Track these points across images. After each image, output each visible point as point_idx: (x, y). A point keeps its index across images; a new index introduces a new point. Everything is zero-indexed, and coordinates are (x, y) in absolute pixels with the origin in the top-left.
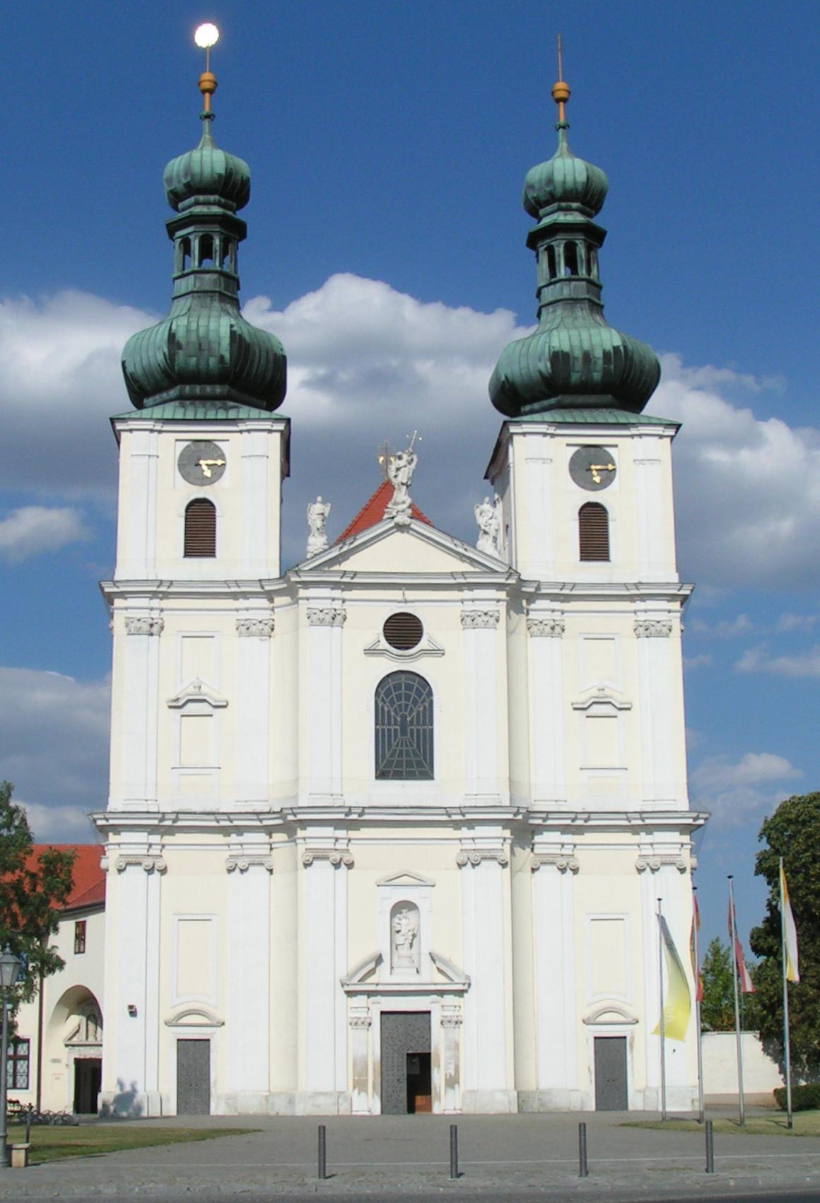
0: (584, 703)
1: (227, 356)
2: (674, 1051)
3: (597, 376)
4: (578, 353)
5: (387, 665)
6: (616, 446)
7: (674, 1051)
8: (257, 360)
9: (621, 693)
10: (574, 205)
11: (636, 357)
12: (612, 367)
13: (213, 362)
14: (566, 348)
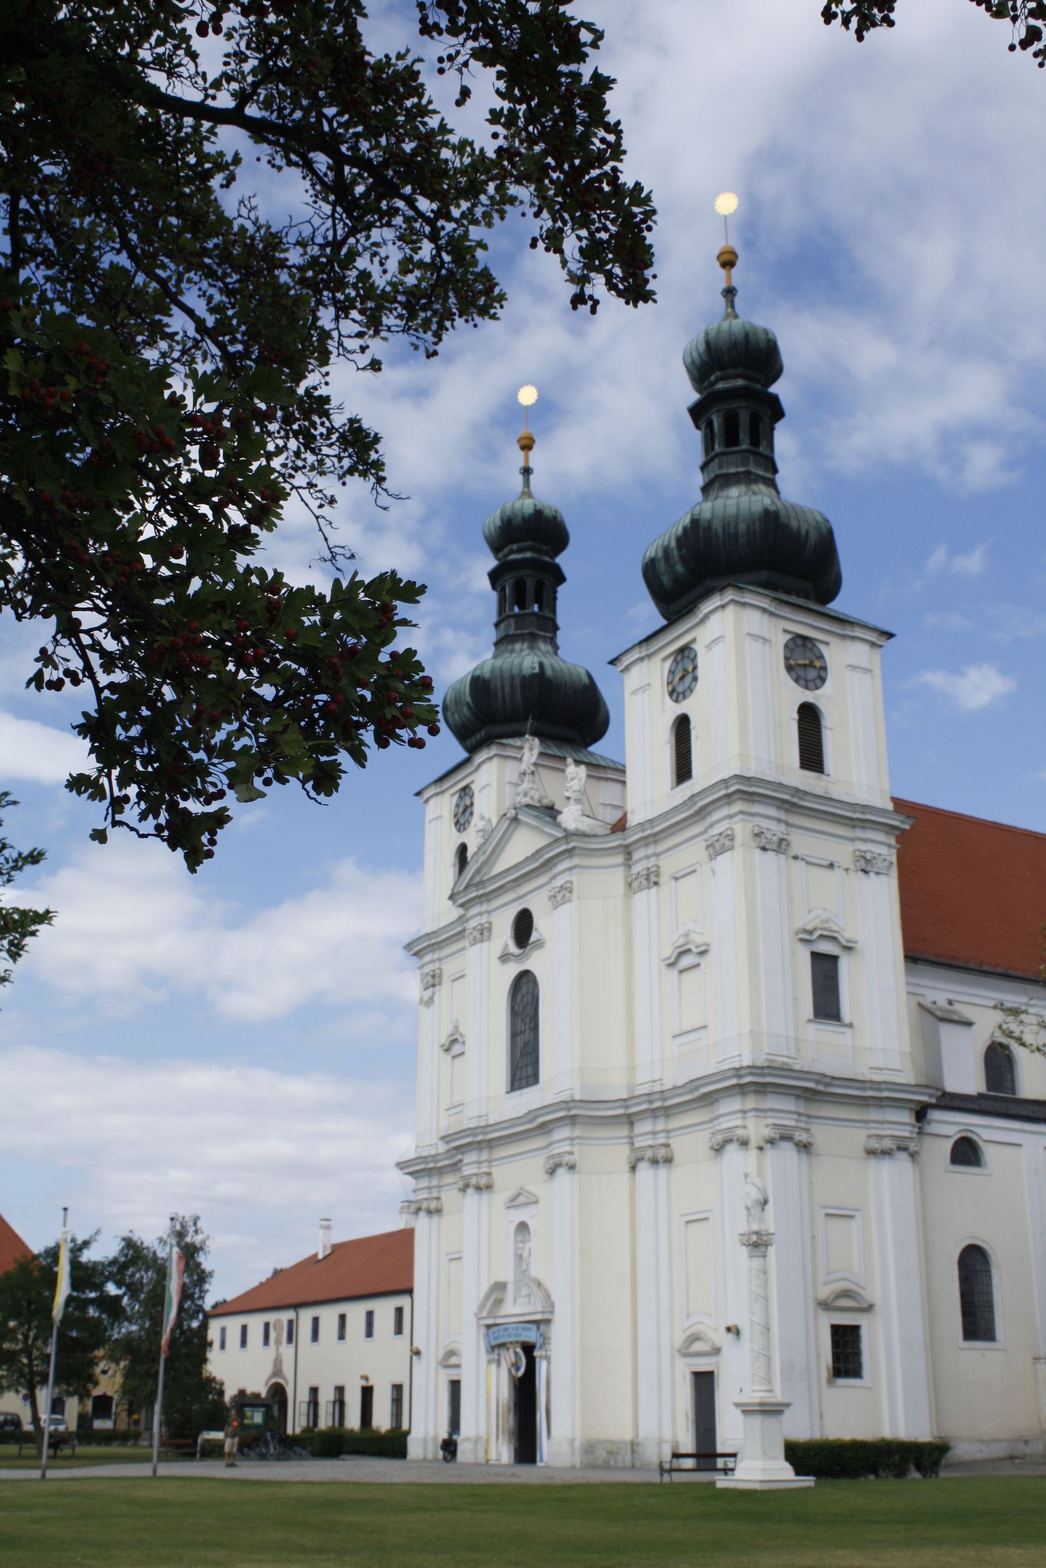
0: (669, 958)
1: (469, 699)
2: (741, 1390)
3: (679, 568)
4: (660, 554)
5: (513, 970)
6: (694, 641)
7: (741, 1390)
8: (499, 693)
9: (702, 934)
10: (712, 378)
11: (717, 525)
12: (685, 551)
13: (465, 710)
14: (653, 555)
